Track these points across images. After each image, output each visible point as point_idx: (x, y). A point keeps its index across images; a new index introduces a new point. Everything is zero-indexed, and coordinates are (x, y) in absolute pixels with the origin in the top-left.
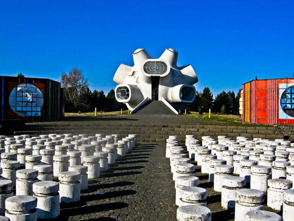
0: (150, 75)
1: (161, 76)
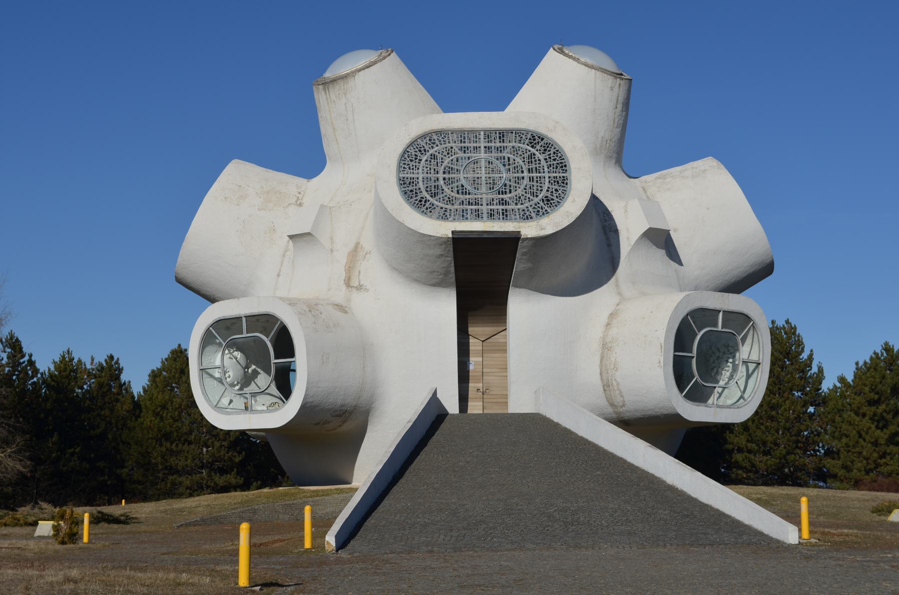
0: (444, 229)
1: (530, 230)
